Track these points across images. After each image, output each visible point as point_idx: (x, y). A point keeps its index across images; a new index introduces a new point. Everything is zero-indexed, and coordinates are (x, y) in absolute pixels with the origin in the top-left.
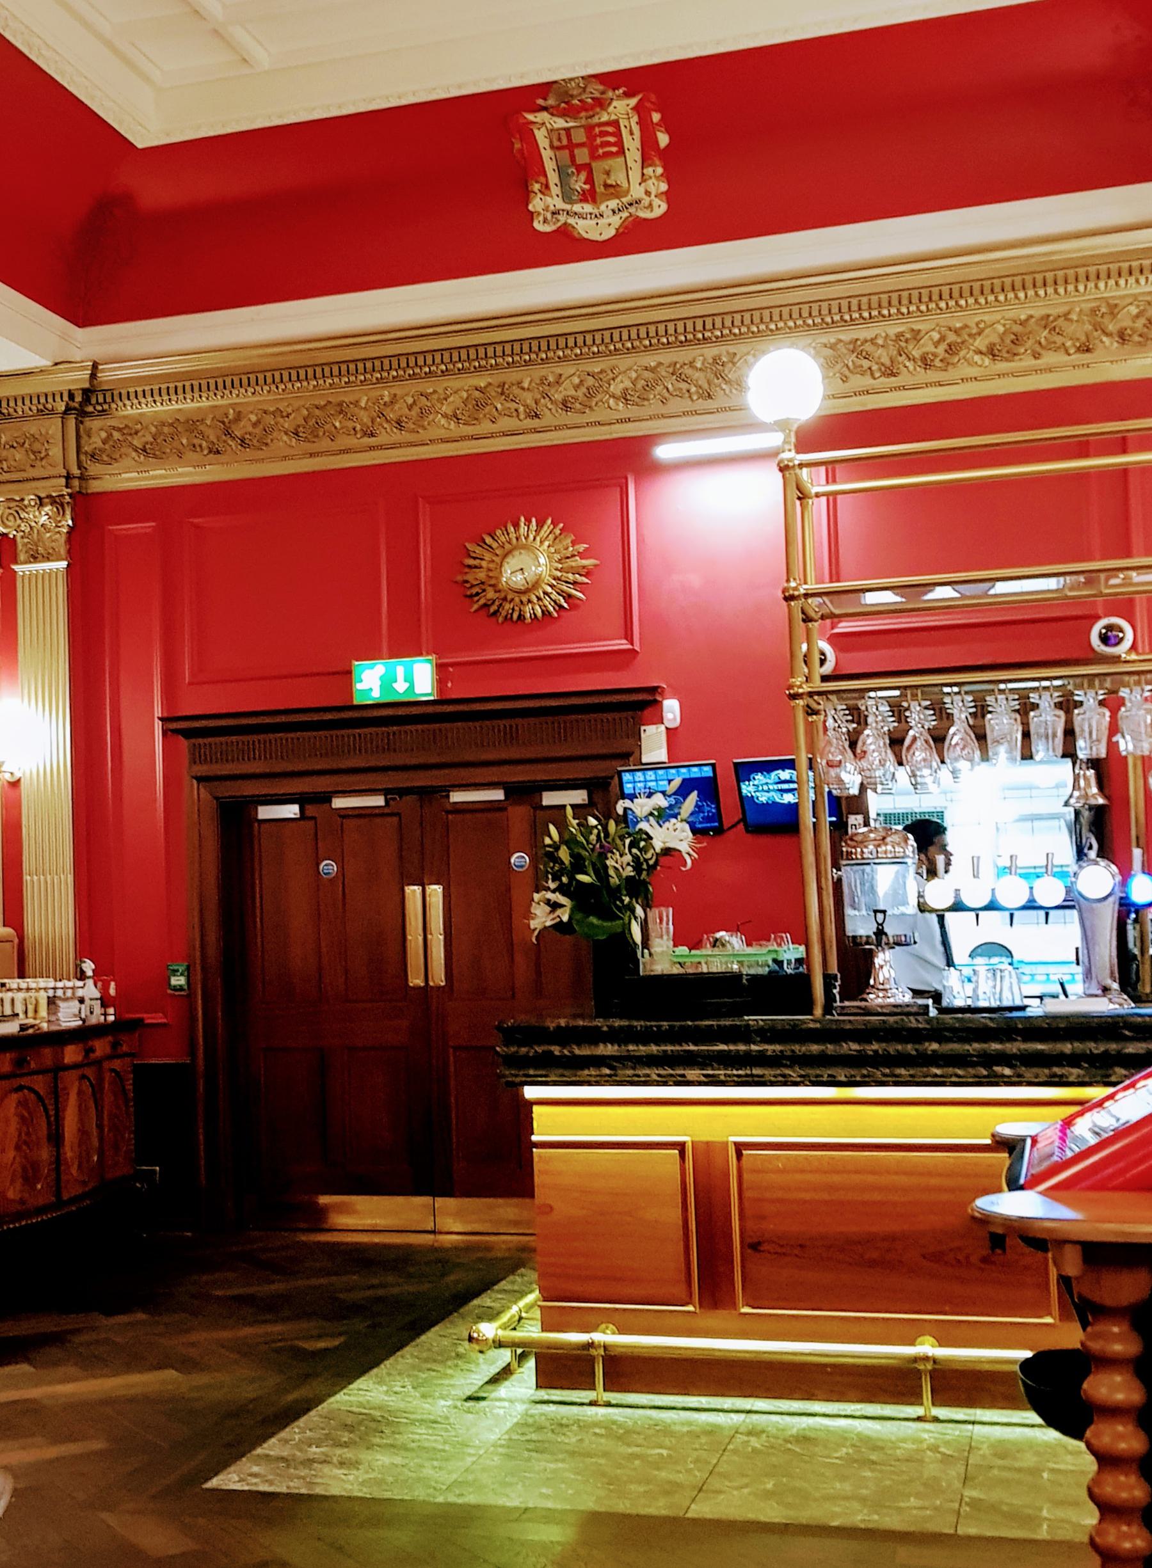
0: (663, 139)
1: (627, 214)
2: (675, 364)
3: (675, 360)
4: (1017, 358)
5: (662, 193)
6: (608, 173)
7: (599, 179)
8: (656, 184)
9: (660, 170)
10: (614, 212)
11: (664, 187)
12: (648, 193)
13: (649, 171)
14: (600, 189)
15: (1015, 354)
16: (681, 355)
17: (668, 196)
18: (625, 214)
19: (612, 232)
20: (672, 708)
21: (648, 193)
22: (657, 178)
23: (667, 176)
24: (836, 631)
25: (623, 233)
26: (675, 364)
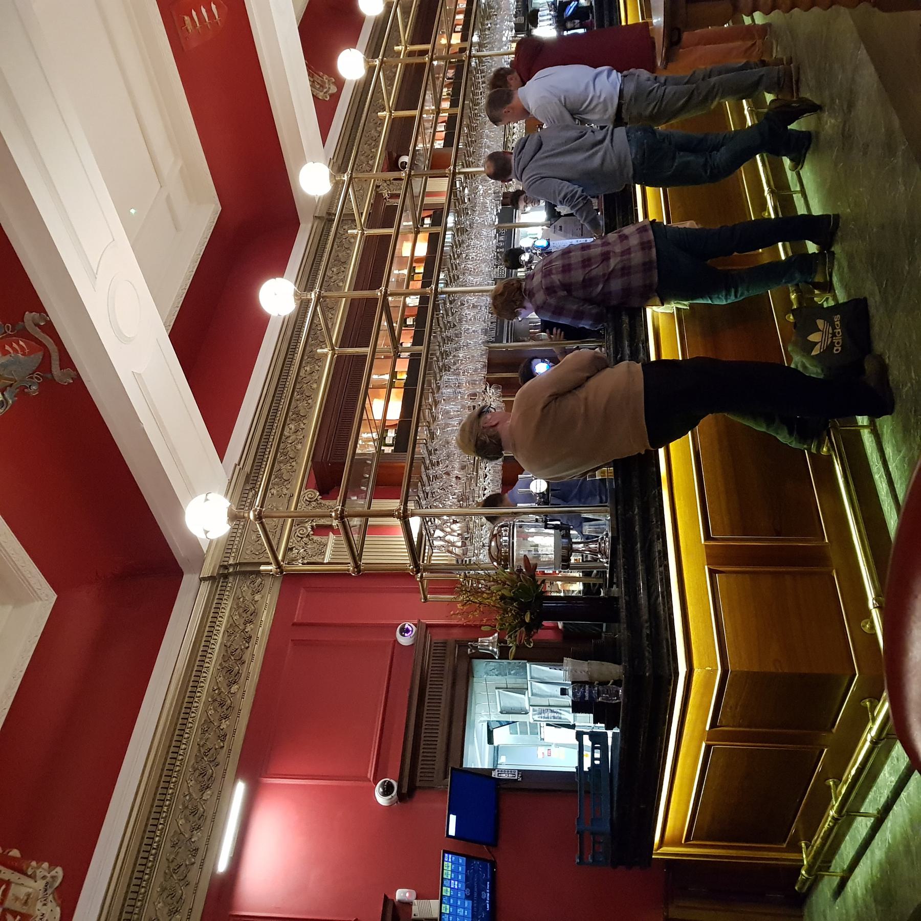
0: (15, 853)
1: (51, 896)
2: (165, 873)
3: (163, 872)
4: (240, 672)
5: (49, 867)
6: (17, 899)
7: (17, 907)
8: (40, 870)
9: (34, 863)
10: (45, 905)
11: (46, 865)
12: (44, 877)
13: (30, 872)
14: (24, 910)
15: (238, 673)
16: (161, 866)
17: (53, 865)
18: (51, 898)
19: (58, 909)
20: (401, 894)
21: (44, 877)
22: (38, 868)
23: (40, 860)
24: (372, 780)
25: (62, 902)
26: (165, 873)
